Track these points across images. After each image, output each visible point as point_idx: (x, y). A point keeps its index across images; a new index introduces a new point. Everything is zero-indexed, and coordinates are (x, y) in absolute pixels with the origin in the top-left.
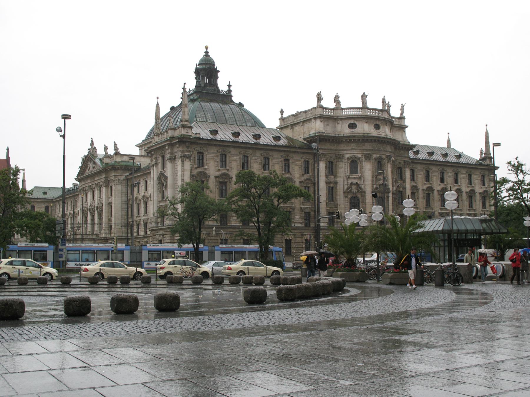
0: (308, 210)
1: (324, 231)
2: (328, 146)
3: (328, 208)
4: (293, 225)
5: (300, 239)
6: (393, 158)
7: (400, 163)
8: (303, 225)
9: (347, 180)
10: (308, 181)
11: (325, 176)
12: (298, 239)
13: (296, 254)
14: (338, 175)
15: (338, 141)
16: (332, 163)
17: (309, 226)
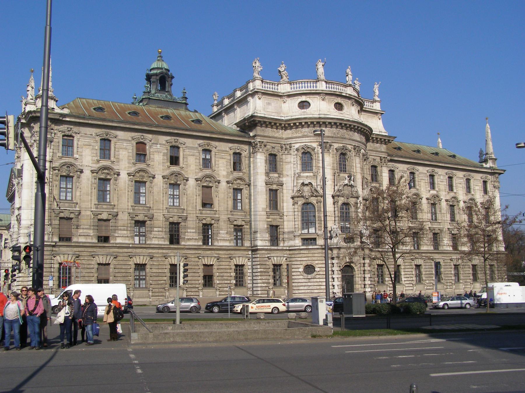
1: (263, 252)
2: (269, 132)
4: (216, 243)
5: (227, 263)
6: (362, 151)
7: (374, 160)
9: (297, 180)
10: (239, 181)
11: (264, 174)
12: (224, 263)
13: (220, 286)
14: (285, 173)
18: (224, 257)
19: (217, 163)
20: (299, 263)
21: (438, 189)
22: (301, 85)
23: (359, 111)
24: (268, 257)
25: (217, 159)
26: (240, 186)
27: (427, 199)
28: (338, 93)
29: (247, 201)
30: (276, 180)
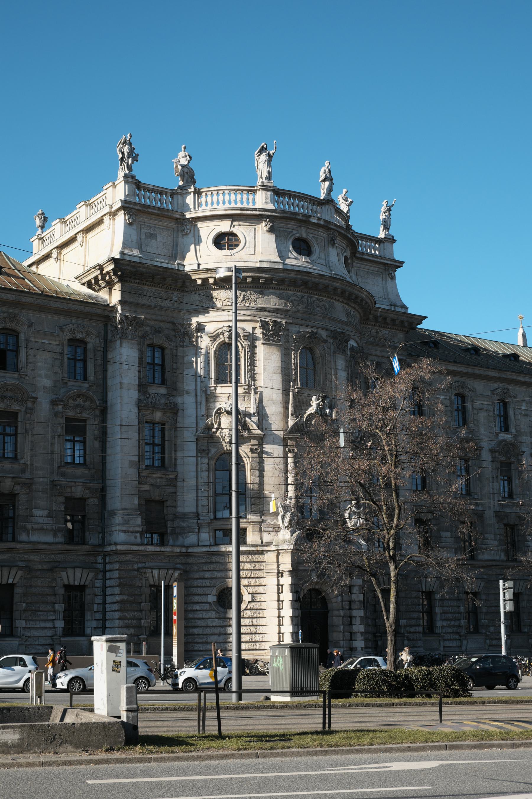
0: (78, 491)
1: (129, 557)
3: (145, 487)
4: (23, 537)
8: (60, 539)
11: (136, 387)
15: (179, 284)
16: (162, 349)
17: (84, 542)
18: (40, 567)
19: (31, 359)
20: (207, 583)
21: (517, 431)
22: (221, 197)
23: (346, 259)
24: (138, 570)
25: (31, 352)
26: (81, 413)
27: (492, 451)
28: (300, 217)
29: (97, 444)
30: (163, 401)
